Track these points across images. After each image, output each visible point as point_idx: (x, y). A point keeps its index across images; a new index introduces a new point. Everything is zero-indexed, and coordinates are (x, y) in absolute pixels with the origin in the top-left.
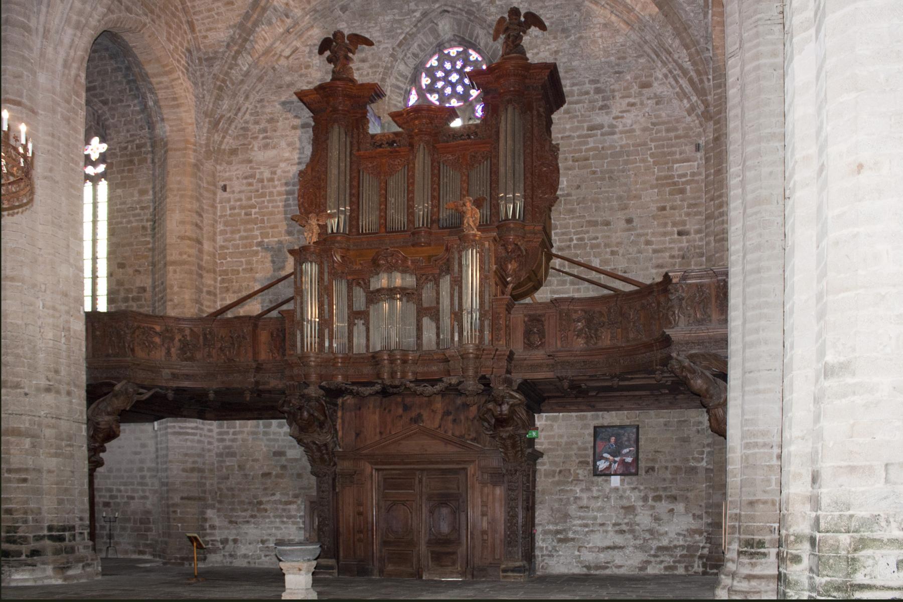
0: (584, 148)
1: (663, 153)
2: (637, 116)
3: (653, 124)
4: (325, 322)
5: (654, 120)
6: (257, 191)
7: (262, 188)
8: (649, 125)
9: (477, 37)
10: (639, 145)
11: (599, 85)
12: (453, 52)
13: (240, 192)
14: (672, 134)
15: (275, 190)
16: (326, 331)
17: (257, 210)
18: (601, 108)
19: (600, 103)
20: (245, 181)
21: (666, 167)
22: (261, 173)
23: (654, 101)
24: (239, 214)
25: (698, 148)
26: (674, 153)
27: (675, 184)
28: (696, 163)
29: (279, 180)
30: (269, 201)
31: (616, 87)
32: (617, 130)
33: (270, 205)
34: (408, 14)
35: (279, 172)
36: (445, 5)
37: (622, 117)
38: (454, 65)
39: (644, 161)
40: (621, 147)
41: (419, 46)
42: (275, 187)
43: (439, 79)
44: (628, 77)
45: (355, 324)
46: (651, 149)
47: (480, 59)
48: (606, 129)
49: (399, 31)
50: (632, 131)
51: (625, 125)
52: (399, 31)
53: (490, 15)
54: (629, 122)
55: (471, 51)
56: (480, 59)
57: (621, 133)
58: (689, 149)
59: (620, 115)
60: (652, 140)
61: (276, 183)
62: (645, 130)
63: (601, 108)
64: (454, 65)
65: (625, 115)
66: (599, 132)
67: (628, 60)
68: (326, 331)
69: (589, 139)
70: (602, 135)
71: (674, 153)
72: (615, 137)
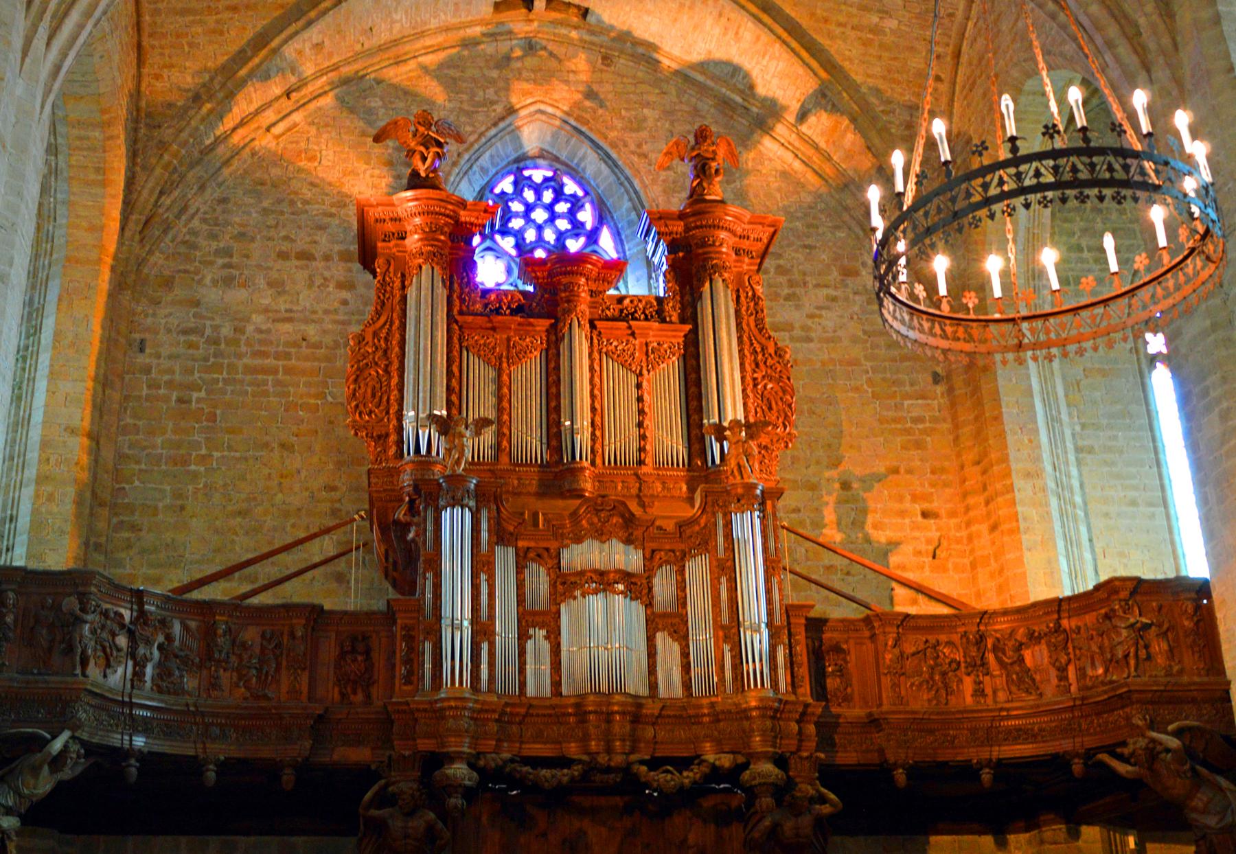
2: (841, 317)
3: (865, 332)
4: (482, 630)
5: (866, 328)
6: (206, 359)
7: (215, 356)
8: (860, 334)
9: (583, 158)
11: (781, 262)
12: (538, 176)
13: (170, 357)
15: (240, 365)
16: (485, 646)
17: (203, 394)
18: (788, 298)
19: (786, 291)
20: (182, 338)
22: (216, 328)
23: (864, 298)
24: (167, 399)
25: (937, 378)
27: (908, 432)
28: (936, 402)
29: (248, 343)
30: (225, 381)
31: (807, 267)
32: (813, 335)
33: (229, 388)
34: (484, 105)
35: (250, 328)
36: (542, 102)
37: (820, 316)
38: (539, 196)
41: (492, 156)
42: (239, 356)
43: (517, 215)
44: (824, 257)
45: (530, 637)
47: (580, 193)
48: (797, 332)
49: (468, 129)
51: (824, 330)
52: (468, 129)
53: (613, 128)
54: (829, 324)
55: (566, 180)
56: (580, 193)
57: (821, 340)
58: (925, 379)
59: (818, 312)
61: (243, 349)
62: (854, 340)
63: (788, 298)
64: (539, 196)
65: (823, 312)
67: (820, 231)
68: (485, 646)
72: (812, 345)
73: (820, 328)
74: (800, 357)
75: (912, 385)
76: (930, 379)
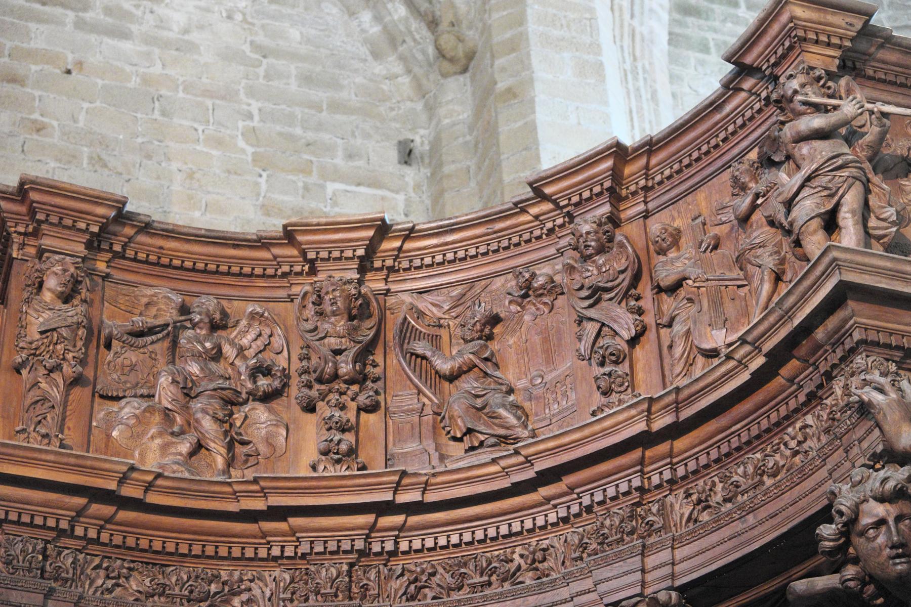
0: (9, 44)
1: (291, 138)
5: (261, 39)
8: (247, 48)
10: (207, 93)
14: (320, 95)
21: (300, 180)
25: (407, 155)
26: (330, 149)
28: (401, 198)
32: (134, 28)
39: (218, 142)
40: (146, 80)
46: (250, 116)
50: (185, 47)
51: (162, 23)
57: (149, 40)
60: (251, 92)
62: (229, 56)
66: (71, 15)
69: (33, 26)
70: (80, 25)
71: (330, 149)
72: (127, 46)
73: (148, 16)
74: (94, 59)
75: (350, 156)
76: (393, 154)
